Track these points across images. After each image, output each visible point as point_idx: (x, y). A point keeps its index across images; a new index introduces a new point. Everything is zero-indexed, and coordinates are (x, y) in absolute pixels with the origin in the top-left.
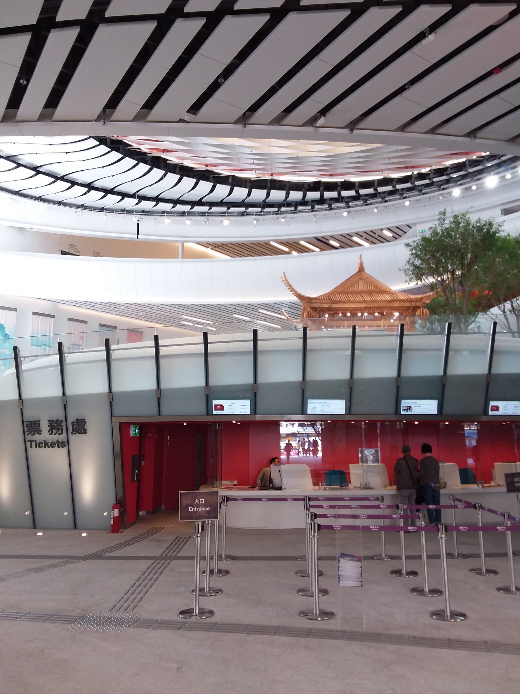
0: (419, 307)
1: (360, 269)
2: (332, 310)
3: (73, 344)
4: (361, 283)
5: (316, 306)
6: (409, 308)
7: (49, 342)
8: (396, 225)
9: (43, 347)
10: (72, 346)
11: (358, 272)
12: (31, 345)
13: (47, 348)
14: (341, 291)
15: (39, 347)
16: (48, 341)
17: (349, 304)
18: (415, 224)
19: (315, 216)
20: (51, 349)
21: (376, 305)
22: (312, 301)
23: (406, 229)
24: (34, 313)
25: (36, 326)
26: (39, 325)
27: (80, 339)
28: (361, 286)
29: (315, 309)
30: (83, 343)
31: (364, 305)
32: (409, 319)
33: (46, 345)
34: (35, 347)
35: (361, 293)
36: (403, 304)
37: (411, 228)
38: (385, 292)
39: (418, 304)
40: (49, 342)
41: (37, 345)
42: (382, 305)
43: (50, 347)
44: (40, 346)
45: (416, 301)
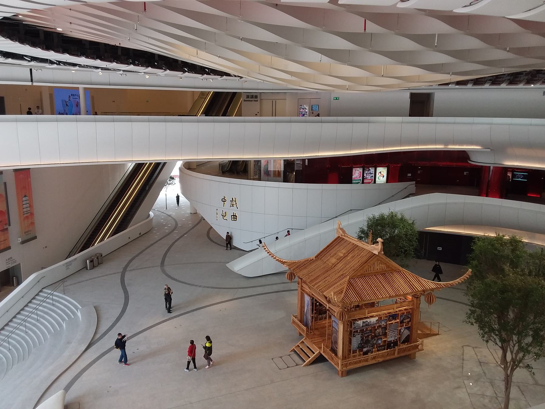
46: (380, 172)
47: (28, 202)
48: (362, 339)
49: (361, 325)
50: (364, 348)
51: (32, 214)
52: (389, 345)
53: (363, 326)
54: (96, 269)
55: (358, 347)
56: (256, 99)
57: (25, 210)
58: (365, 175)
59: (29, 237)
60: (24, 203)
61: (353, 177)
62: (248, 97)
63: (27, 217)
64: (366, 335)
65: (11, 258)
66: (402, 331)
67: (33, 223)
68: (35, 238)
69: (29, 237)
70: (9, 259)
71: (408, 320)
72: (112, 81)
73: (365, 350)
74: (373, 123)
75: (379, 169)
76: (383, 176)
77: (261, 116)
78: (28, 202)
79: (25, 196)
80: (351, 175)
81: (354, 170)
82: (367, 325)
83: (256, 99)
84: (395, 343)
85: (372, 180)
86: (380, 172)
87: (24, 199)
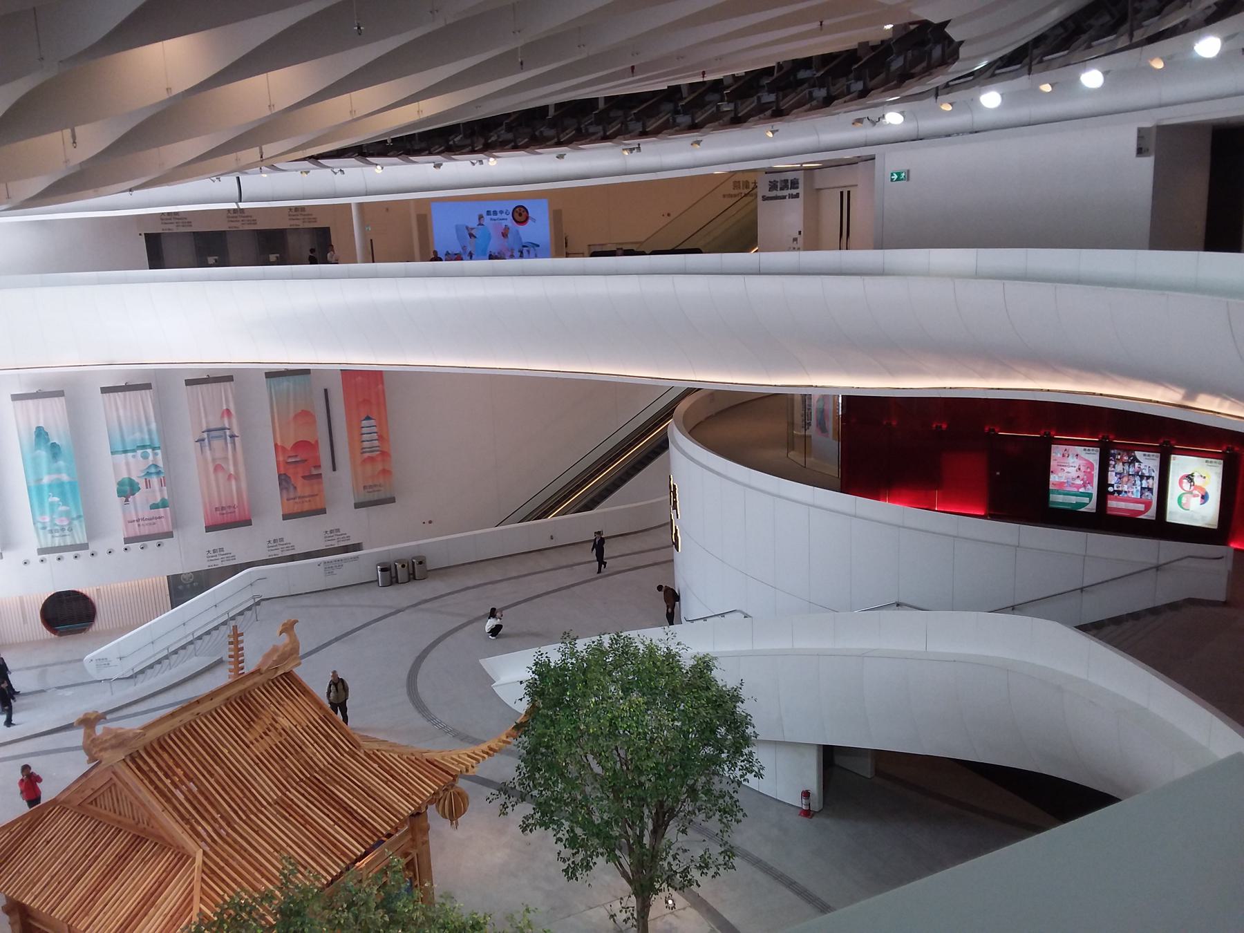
3: (209, 431)
7: (151, 439)
9: (140, 452)
10: (205, 435)
12: (112, 453)
13: (149, 451)
15: (130, 455)
16: (147, 437)
20: (159, 451)
24: (105, 390)
25: (115, 414)
26: (121, 412)
27: (222, 416)
30: (230, 423)
33: (144, 447)
34: (121, 458)
40: (151, 439)
41: (125, 452)
43: (154, 449)
44: (134, 451)
46: (1190, 478)
47: (374, 429)
51: (384, 454)
54: (397, 586)
56: (794, 192)
57: (366, 444)
58: (1112, 478)
59: (375, 496)
60: (365, 430)
61: (1054, 478)
62: (773, 186)
63: (372, 459)
65: (338, 530)
67: (385, 472)
68: (392, 500)
69: (376, 498)
70: (331, 532)
72: (374, 184)
74: (899, 275)
75: (1181, 465)
76: (1204, 498)
77: (809, 247)
78: (374, 429)
79: (368, 418)
80: (1046, 471)
81: (1057, 452)
83: (794, 192)
85: (1148, 505)
86: (1190, 478)
87: (365, 423)
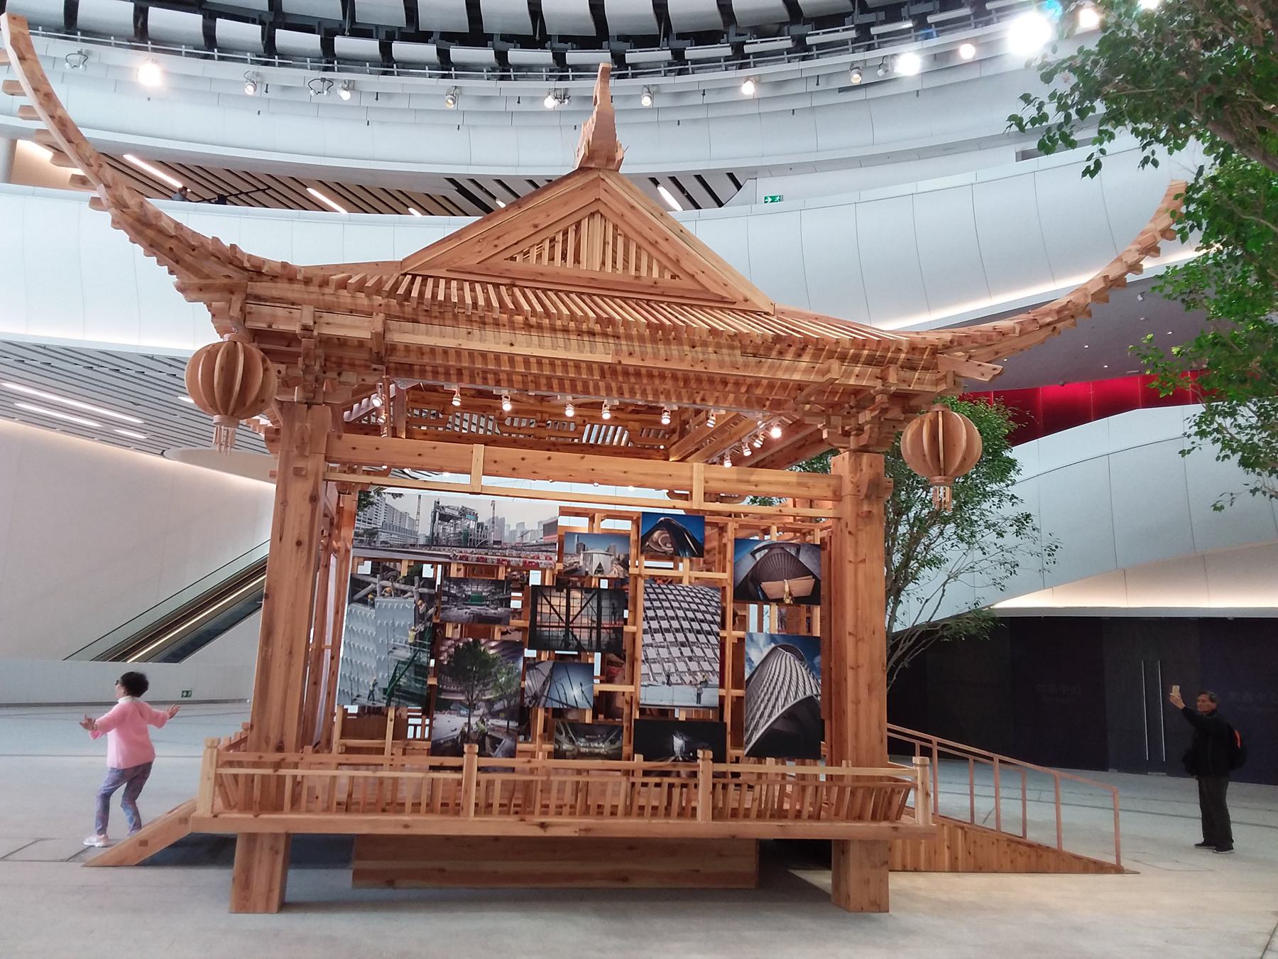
0: (906, 403)
1: (590, 156)
2: (406, 370)
4: (593, 235)
5: (288, 322)
6: (860, 397)
8: (699, 167)
11: (582, 169)
14: (471, 261)
17: (506, 335)
18: (754, 173)
19: (456, 95)
21: (679, 359)
22: (262, 288)
23: (723, 187)
28: (594, 254)
29: (275, 344)
31: (601, 354)
32: (856, 468)
35: (593, 288)
36: (836, 370)
37: (739, 187)
38: (722, 300)
39: (919, 382)
42: (716, 363)
45: (910, 366)
48: (431, 636)
49: (424, 529)
50: (445, 706)
52: (654, 731)
53: (433, 541)
55: (394, 691)
64: (464, 612)
66: (755, 655)
71: (801, 586)
73: (450, 723)
82: (466, 540)
84: (709, 732)
